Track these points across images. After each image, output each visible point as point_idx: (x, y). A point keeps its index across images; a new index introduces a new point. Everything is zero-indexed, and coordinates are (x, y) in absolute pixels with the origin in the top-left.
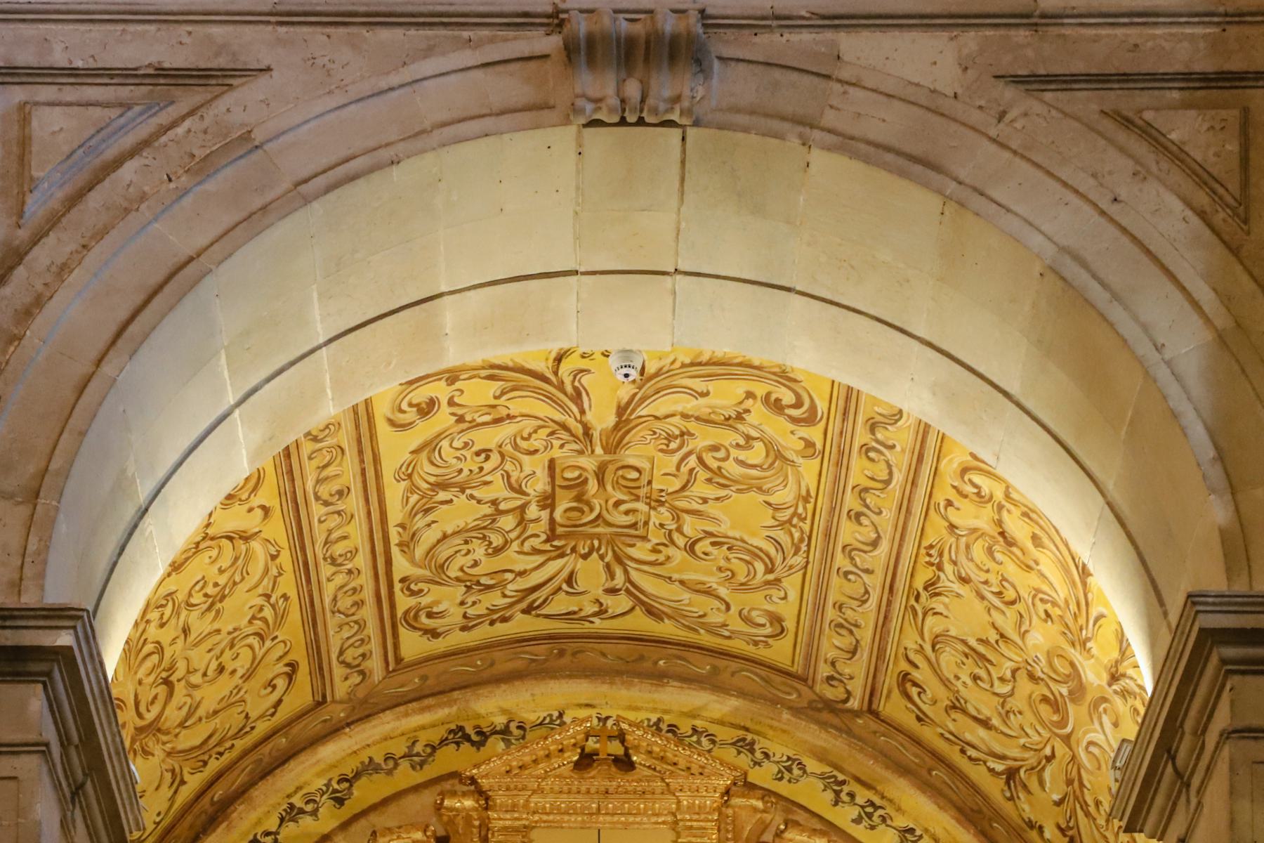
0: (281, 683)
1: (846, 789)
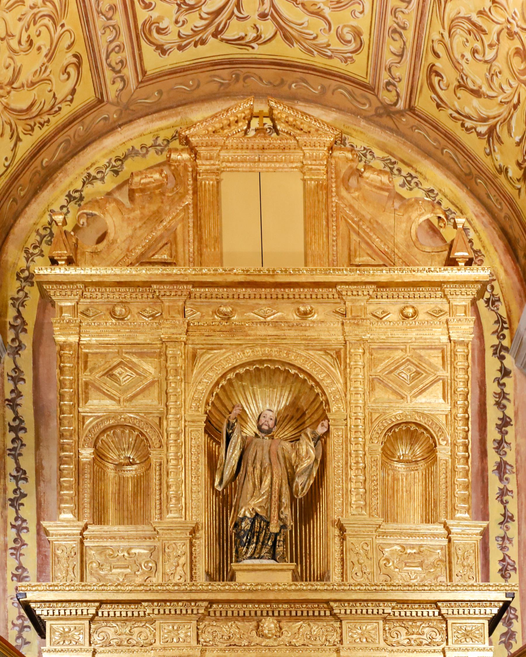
1: (396, 167)
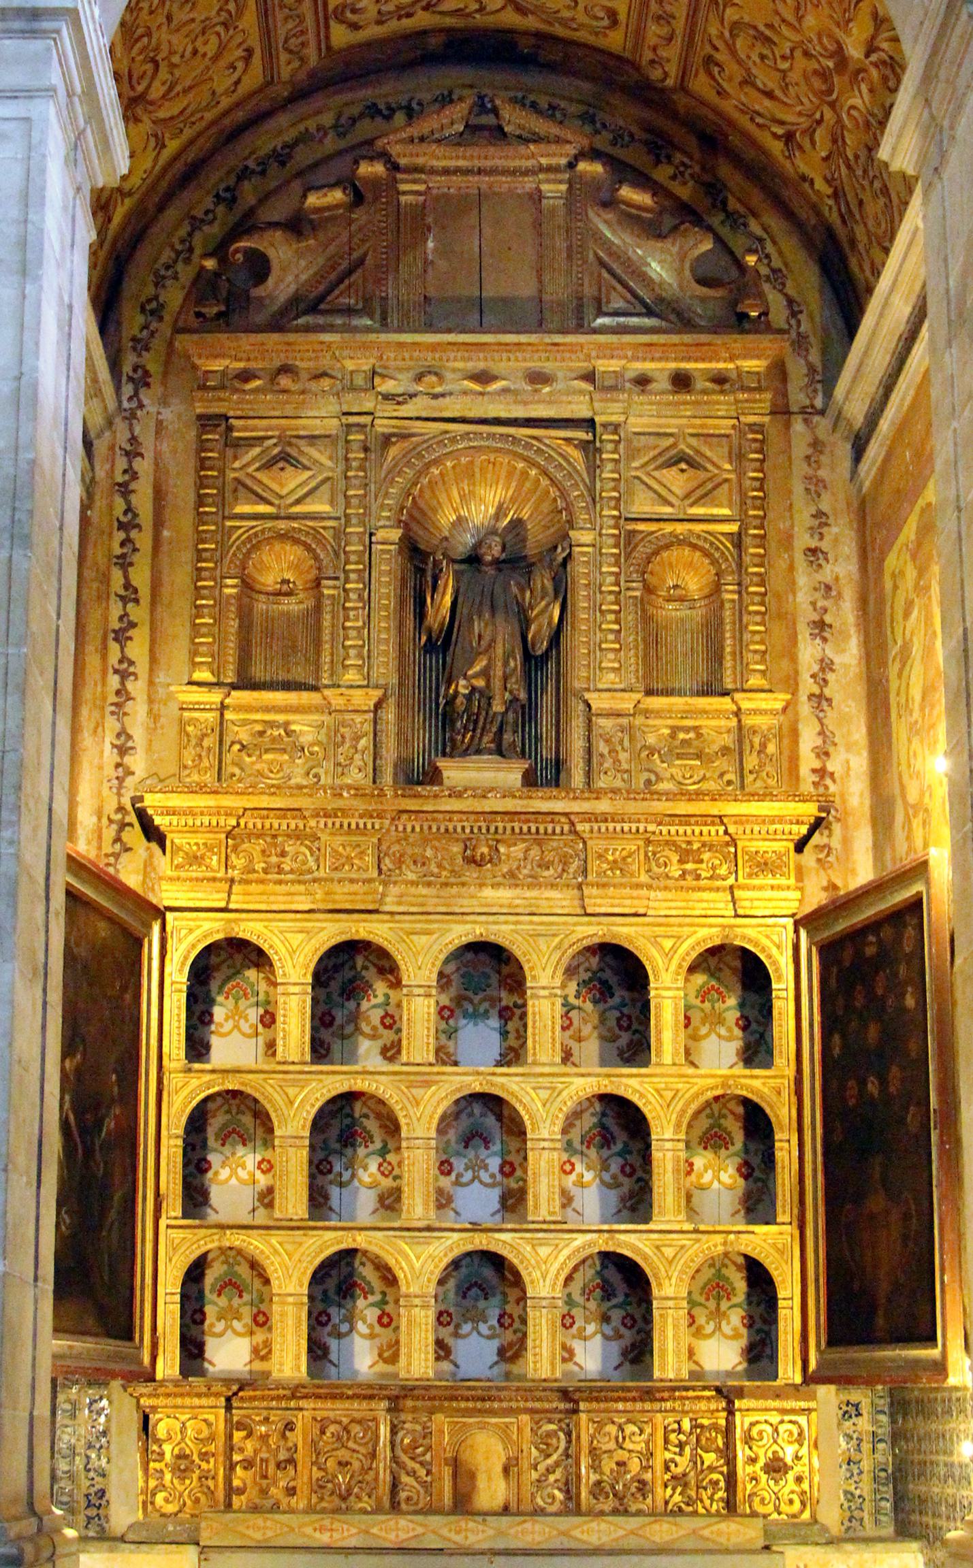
0: (240, 65)
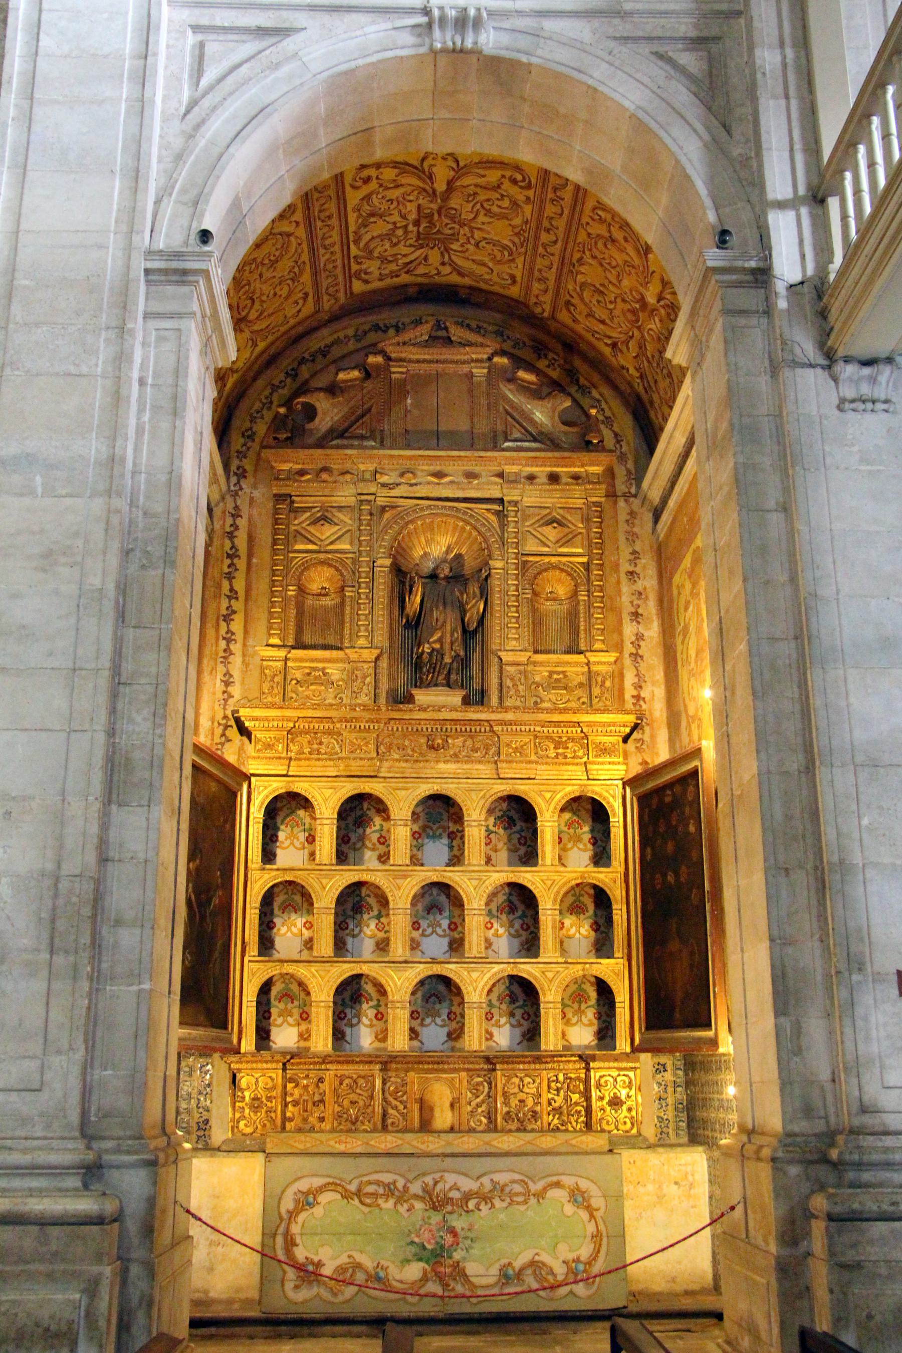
0: (301, 302)
